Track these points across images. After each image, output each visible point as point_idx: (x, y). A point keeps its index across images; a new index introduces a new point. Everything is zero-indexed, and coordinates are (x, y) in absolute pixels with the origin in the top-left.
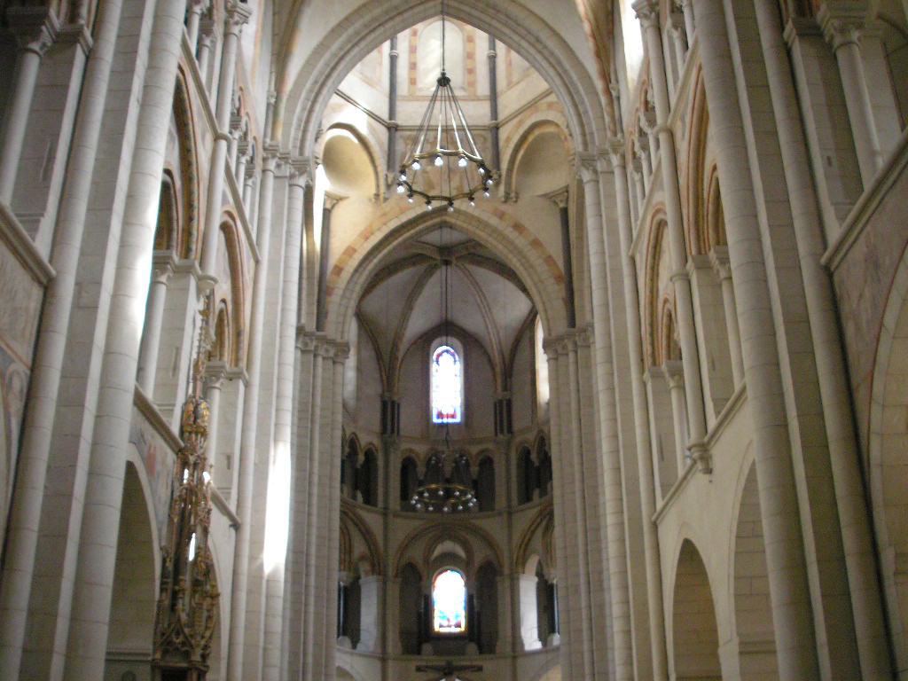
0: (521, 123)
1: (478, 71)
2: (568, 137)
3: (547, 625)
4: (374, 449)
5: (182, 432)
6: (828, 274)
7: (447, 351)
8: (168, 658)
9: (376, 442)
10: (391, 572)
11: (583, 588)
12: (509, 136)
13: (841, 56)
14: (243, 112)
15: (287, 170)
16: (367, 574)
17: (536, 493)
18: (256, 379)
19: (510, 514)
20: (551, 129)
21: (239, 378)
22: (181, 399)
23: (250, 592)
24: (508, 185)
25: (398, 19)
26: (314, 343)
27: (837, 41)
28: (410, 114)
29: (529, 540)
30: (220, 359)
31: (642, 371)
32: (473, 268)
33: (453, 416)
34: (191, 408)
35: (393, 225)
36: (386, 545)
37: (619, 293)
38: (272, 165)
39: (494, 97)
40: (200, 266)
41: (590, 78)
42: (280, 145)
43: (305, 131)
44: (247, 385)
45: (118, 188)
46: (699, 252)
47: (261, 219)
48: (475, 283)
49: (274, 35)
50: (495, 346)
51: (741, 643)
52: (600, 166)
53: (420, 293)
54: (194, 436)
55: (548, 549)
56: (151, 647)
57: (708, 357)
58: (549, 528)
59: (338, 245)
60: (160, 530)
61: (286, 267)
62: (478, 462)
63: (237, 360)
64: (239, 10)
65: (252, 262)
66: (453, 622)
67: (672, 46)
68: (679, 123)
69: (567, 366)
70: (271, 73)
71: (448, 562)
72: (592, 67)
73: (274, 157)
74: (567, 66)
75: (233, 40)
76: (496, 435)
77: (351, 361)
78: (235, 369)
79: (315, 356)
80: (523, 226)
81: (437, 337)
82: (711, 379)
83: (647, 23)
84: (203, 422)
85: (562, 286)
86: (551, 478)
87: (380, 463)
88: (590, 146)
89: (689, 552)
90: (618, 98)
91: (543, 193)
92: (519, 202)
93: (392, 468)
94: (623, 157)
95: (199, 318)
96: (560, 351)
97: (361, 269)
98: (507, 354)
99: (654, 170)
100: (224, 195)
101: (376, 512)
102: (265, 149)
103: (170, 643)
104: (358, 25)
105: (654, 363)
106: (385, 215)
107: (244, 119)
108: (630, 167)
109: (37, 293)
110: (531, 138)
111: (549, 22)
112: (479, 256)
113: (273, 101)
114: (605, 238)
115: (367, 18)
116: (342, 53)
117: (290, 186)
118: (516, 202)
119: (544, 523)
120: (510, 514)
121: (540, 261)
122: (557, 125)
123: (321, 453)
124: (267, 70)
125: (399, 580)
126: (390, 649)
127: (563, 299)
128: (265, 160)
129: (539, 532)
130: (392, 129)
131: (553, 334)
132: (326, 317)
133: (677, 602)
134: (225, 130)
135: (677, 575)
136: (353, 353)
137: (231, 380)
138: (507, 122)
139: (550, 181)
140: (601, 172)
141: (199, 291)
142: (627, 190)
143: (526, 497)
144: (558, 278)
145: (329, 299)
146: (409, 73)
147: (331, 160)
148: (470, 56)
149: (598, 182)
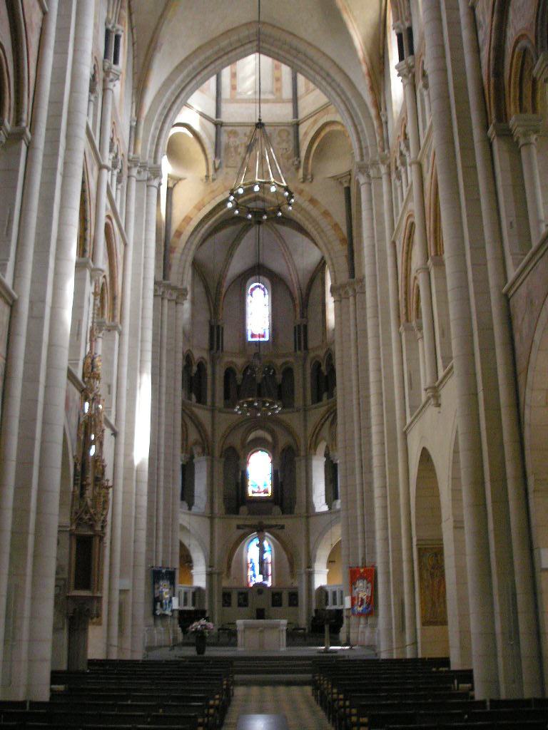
0: (315, 121)
3: (332, 495)
4: (204, 362)
5: (83, 377)
6: (506, 299)
7: (259, 287)
8: (80, 529)
9: (206, 355)
10: (217, 454)
11: (357, 470)
12: (307, 131)
13: (523, 153)
14: (115, 140)
15: (145, 175)
16: (198, 454)
17: (325, 396)
18: (127, 330)
19: (305, 411)
20: (338, 128)
21: (115, 330)
22: (82, 356)
23: (125, 479)
24: (306, 169)
25: (225, 58)
26: (162, 290)
27: (522, 141)
28: (232, 113)
29: (320, 430)
30: (102, 317)
31: (399, 325)
32: (279, 227)
33: (263, 336)
34: (89, 361)
36: (213, 435)
37: (384, 269)
38: (134, 172)
39: (295, 100)
40: (92, 260)
41: (366, 105)
42: (140, 157)
43: (157, 145)
44: (121, 334)
45: (52, 237)
46: (436, 254)
47: (127, 213)
48: (281, 237)
49: (134, 74)
50: (295, 285)
51: (454, 521)
52: (372, 172)
53: (238, 245)
54: (92, 381)
55: (333, 437)
56: (69, 522)
57: (439, 328)
58: (334, 422)
59: (179, 215)
60: (72, 445)
61: (146, 247)
62: (281, 371)
63: (113, 317)
64: (112, 70)
65: (122, 245)
66: (262, 489)
67: (422, 100)
68: (425, 160)
69: (348, 307)
70: (132, 103)
71: (258, 444)
72: (368, 97)
73: (136, 166)
74: (349, 94)
75: (109, 93)
76: (296, 351)
77: (187, 305)
78: (112, 324)
79: (162, 299)
81: (248, 279)
82: (441, 343)
83: (406, 81)
84: (97, 370)
85: (346, 247)
86: (335, 385)
87: (209, 371)
88: (365, 158)
89: (425, 456)
90: (386, 123)
91: (330, 175)
93: (217, 376)
94: (389, 167)
95: (92, 297)
96: (343, 296)
97: (196, 233)
98: (304, 291)
99: (405, 197)
100: (106, 206)
101: (207, 410)
102: (129, 160)
103: (81, 519)
104: (196, 62)
105: (407, 320)
106: (213, 191)
107: (116, 142)
108: (394, 176)
109: (7, 310)
110: (323, 134)
113: (134, 124)
114: (375, 226)
115: (202, 57)
117: (147, 186)
118: (311, 182)
119: (330, 419)
120: (305, 411)
121: (329, 227)
122: (342, 125)
123: (168, 371)
124: (130, 101)
125: (223, 459)
126: (216, 511)
128: (129, 168)
129: (328, 423)
130: (218, 125)
131: (339, 283)
132: (170, 269)
133: (418, 488)
134: (108, 163)
135: (419, 470)
136: (189, 297)
137: (109, 331)
138: (305, 121)
139: (336, 166)
140: (373, 178)
141: (92, 277)
142: (390, 192)
143: (317, 398)
144: (343, 241)
145: (172, 256)
146: (231, 80)
147: (174, 151)
148: (278, 79)
149: (370, 184)
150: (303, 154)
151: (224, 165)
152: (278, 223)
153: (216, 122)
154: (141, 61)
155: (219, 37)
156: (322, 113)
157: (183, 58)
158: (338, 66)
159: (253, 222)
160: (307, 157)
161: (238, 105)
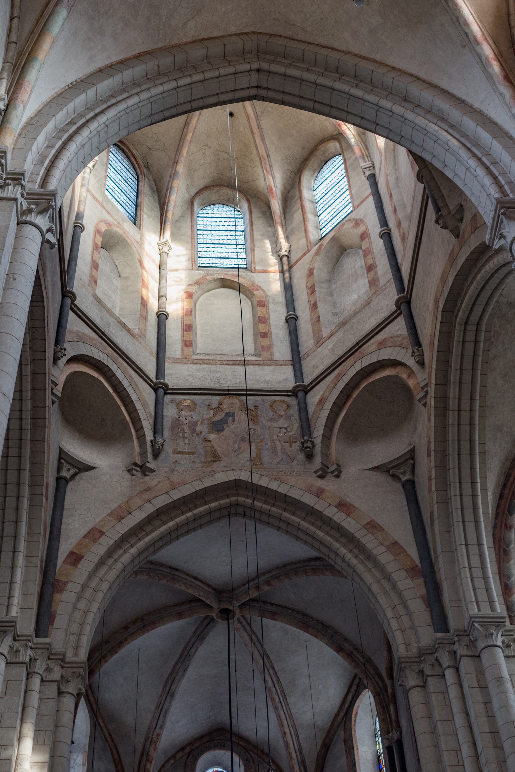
1: (274, 336)
2: (415, 368)
24: (326, 455)
35: (161, 502)
49: (8, 43)
53: (185, 670)
79: (29, 675)
80: (350, 505)
91: (375, 465)
92: (343, 475)
97: (111, 561)
111: (422, 75)
112: (272, 604)
116: (113, 101)
117: (19, 223)
118: (338, 476)
122: (395, 363)
127: (422, 598)
146: (183, 335)
150: (318, 433)
151: (168, 449)
152: (263, 614)
153: (155, 384)
154: (28, 27)
155: (186, 44)
156: (351, 360)
157: (115, 59)
158: (424, 81)
159: (214, 615)
160: (327, 437)
161: (195, 367)
